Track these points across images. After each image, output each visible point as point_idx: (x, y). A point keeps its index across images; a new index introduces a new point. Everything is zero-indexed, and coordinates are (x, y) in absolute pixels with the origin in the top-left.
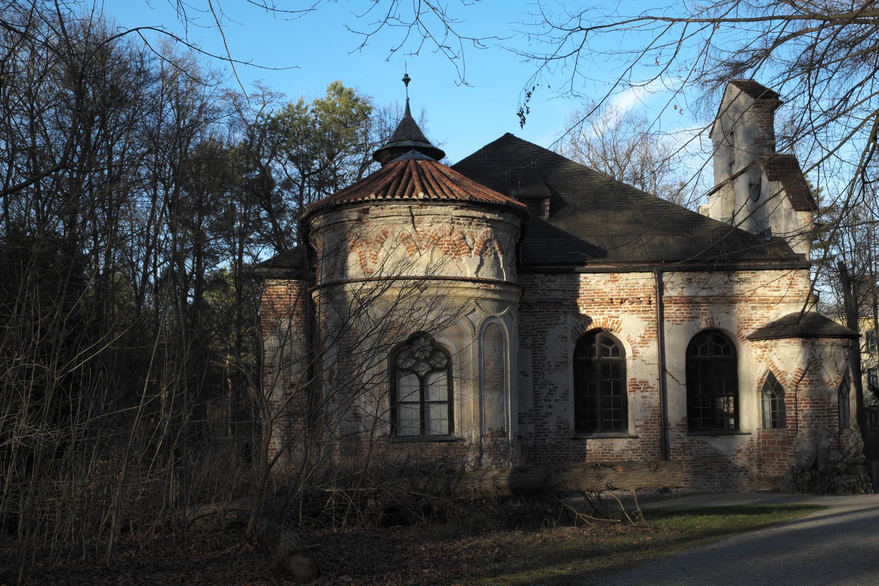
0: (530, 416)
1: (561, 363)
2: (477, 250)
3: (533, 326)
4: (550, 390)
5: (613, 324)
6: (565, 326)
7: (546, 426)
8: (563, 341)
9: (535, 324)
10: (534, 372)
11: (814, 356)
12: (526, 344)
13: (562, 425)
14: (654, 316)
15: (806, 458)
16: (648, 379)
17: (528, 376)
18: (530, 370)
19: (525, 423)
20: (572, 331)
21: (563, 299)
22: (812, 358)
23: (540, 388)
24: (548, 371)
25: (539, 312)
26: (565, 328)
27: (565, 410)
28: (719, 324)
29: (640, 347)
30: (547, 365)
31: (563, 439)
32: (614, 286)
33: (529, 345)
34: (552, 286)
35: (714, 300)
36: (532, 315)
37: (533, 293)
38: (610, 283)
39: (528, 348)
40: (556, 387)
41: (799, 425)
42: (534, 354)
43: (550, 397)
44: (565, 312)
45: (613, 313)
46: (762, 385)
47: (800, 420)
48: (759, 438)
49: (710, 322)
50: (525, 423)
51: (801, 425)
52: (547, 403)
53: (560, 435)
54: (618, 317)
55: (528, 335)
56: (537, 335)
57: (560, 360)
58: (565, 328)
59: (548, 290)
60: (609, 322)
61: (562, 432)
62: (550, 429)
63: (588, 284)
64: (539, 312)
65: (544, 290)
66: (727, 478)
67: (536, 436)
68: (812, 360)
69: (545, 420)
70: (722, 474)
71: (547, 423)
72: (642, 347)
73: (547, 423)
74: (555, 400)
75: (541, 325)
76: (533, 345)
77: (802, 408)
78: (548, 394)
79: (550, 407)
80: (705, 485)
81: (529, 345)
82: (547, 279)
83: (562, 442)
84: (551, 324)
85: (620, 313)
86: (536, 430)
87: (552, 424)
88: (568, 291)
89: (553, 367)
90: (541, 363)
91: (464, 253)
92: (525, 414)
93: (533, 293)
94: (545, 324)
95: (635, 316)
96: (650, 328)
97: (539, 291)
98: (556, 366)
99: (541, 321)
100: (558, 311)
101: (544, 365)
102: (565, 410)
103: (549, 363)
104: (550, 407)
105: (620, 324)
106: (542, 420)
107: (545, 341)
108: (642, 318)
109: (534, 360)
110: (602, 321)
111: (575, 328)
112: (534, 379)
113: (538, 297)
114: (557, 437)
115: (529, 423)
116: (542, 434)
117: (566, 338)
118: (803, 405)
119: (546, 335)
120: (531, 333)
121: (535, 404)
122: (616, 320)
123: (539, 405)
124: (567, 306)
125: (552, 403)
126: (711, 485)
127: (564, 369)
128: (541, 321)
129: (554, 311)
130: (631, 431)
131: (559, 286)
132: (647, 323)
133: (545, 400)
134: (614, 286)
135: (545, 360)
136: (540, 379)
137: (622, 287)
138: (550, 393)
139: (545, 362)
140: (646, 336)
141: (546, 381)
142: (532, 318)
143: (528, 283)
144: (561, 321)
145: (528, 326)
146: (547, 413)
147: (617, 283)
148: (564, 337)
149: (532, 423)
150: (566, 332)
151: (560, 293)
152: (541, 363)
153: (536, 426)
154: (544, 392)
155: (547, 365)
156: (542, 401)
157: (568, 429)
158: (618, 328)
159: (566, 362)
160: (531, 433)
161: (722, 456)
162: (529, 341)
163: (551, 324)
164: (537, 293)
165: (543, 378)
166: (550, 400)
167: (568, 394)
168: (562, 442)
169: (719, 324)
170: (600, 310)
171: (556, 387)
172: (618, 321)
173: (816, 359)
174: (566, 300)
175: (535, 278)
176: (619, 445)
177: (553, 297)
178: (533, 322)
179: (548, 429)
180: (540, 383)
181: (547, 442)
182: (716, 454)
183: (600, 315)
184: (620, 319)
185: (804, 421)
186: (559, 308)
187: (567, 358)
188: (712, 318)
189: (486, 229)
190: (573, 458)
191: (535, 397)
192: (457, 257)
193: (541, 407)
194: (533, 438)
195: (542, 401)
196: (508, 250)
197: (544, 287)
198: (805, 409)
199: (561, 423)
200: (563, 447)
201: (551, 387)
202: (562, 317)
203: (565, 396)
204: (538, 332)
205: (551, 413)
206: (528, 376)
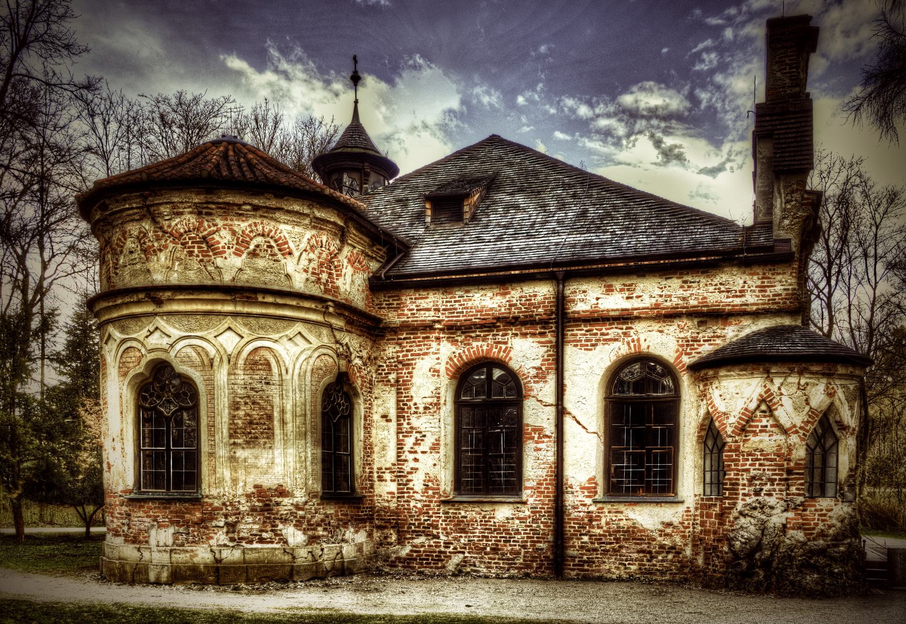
0: (393, 472)
1: (431, 404)
2: (236, 249)
3: (398, 357)
4: (417, 439)
5: (499, 352)
6: (437, 356)
7: (411, 485)
8: (433, 376)
9: (401, 355)
10: (398, 417)
11: (769, 390)
12: (389, 381)
13: (430, 484)
14: (554, 339)
15: (743, 540)
16: (544, 425)
17: (389, 421)
18: (393, 414)
19: (386, 481)
20: (447, 363)
21: (434, 322)
22: (766, 392)
23: (404, 436)
24: (415, 415)
25: (405, 339)
26: (438, 359)
27: (435, 465)
28: (648, 347)
29: (534, 382)
30: (413, 407)
31: (431, 502)
32: (504, 301)
33: (392, 381)
34: (423, 304)
35: (640, 313)
36: (397, 344)
37: (399, 315)
38: (499, 297)
39: (392, 386)
40: (424, 436)
41: (741, 492)
42: (398, 393)
43: (416, 448)
44: (438, 339)
45: (499, 338)
46: (703, 433)
47: (744, 485)
48: (696, 509)
49: (635, 346)
50: (386, 481)
51: (746, 492)
52: (412, 456)
53: (427, 497)
54: (506, 343)
55: (392, 370)
56: (402, 369)
57: (430, 400)
58: (438, 359)
59: (418, 310)
60: (494, 350)
61: (430, 492)
62: (416, 489)
63: (470, 300)
64: (405, 339)
65: (413, 310)
66: (648, 561)
67: (398, 497)
68: (765, 396)
69: (410, 477)
70: (641, 555)
71: (411, 481)
72: (537, 382)
73: (411, 481)
74: (423, 452)
75: (407, 356)
76: (397, 381)
77: (747, 467)
78: (415, 444)
79: (416, 460)
80: (618, 568)
81: (392, 381)
82: (417, 296)
83: (429, 506)
84: (419, 355)
85: (509, 337)
86: (398, 489)
87: (417, 482)
88: (444, 310)
89: (421, 410)
90: (406, 405)
91: (215, 254)
92: (386, 469)
93: (399, 315)
94: (412, 355)
95: (530, 340)
96: (549, 356)
97: (406, 312)
98: (426, 408)
99: (407, 351)
100: (428, 337)
101: (409, 408)
102: (435, 465)
103: (415, 404)
104: (416, 460)
105: (510, 351)
106: (405, 476)
107: (411, 377)
108: (539, 342)
109: (398, 401)
110: (485, 348)
111: (451, 359)
112: (398, 425)
113: (405, 319)
114: (424, 498)
115: (391, 481)
116: (406, 495)
117: (438, 371)
118: (750, 462)
119: (413, 368)
120: (396, 366)
121: (398, 456)
122: (504, 347)
123: (403, 458)
124: (440, 329)
125: (419, 456)
126: (626, 568)
127: (435, 412)
128: (407, 351)
129: (424, 338)
130: (526, 494)
131: (432, 304)
132: (546, 349)
133: (410, 452)
134: (504, 301)
135: (411, 400)
136: (405, 425)
137: (514, 302)
138: (417, 443)
139: (411, 404)
140: (544, 368)
141: (411, 428)
142: (398, 348)
143: (395, 302)
144: (431, 350)
145: (393, 358)
146: (412, 469)
147: (508, 296)
148: (435, 371)
149: (394, 481)
150: (439, 364)
151: (432, 313)
152: (406, 405)
153: (399, 484)
154: (409, 442)
155: (413, 407)
156: (407, 453)
157: (439, 489)
158: (506, 357)
159: (437, 404)
160: (393, 493)
161: (644, 530)
162: (392, 377)
163: (419, 355)
164: (403, 315)
165: (408, 424)
166: (416, 452)
167: (438, 444)
168: (429, 506)
169: (648, 347)
170: (482, 334)
171: (424, 436)
172: (507, 348)
173: (772, 394)
174: (439, 322)
175: (404, 295)
176: (502, 513)
177: (423, 318)
178: (397, 352)
179: (412, 489)
180: (404, 430)
181: (412, 504)
182: (635, 527)
183: (483, 341)
184: (509, 345)
185: (750, 485)
186: (430, 333)
187: (439, 398)
188: (638, 340)
189: (255, 221)
190: (444, 526)
191: (398, 449)
192: (206, 259)
193: (406, 461)
194: (395, 500)
195: (407, 453)
196: (305, 250)
197: (413, 306)
198: (752, 468)
199: (429, 481)
200: (431, 512)
201: (418, 436)
202: (434, 345)
203: (435, 448)
204: (404, 365)
205: (417, 469)
206: (389, 421)
